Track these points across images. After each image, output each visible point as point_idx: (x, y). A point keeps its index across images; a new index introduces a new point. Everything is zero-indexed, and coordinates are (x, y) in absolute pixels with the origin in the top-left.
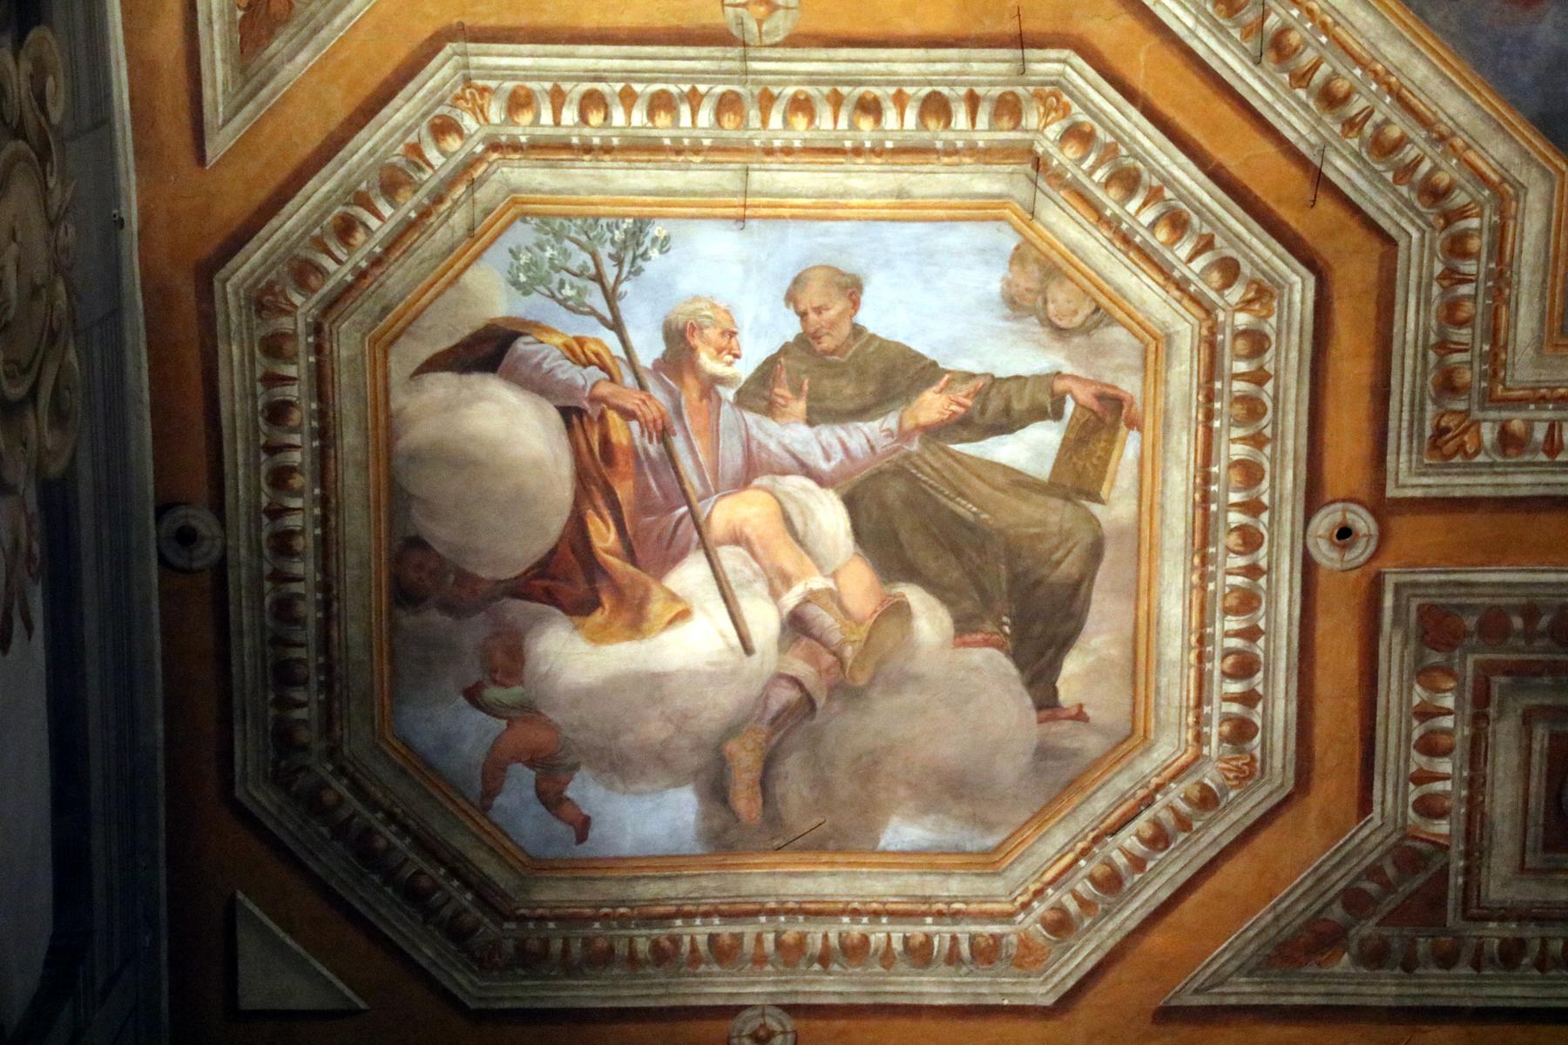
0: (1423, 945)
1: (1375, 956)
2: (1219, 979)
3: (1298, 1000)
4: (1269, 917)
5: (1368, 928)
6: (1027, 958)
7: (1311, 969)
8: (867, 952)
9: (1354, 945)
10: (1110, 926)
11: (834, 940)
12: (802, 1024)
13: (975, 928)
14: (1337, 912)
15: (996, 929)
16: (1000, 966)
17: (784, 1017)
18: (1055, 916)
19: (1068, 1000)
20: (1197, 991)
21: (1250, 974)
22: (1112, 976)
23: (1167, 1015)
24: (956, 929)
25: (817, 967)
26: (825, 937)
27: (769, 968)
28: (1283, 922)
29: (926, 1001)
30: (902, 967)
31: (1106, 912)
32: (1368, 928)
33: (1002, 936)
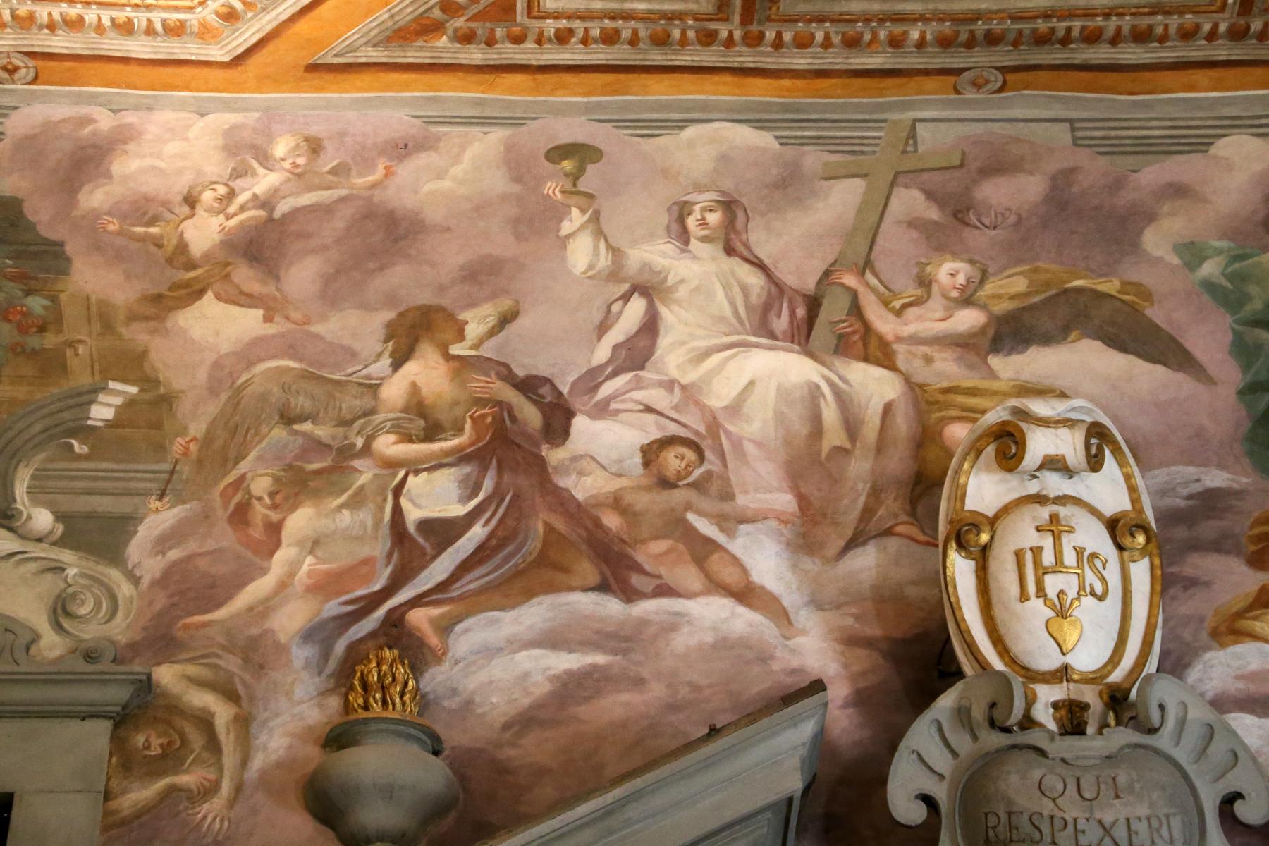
0: (499, 32)
1: (467, 38)
2: (352, 49)
3: (411, 60)
4: (386, 16)
5: (460, 23)
6: (205, 34)
7: (420, 43)
8: (84, 25)
9: (450, 32)
10: (268, 17)
11: (56, 16)
12: (40, 63)
13: (165, 15)
14: (437, 13)
15: (182, 16)
16: (185, 38)
17: (26, 59)
18: (225, 10)
19: (238, 60)
20: (335, 55)
21: (374, 46)
22: (271, 47)
23: (313, 68)
24: (150, 15)
25: (46, 31)
26: (50, 14)
27: (8, 30)
28: (397, 18)
29: (133, 55)
30: (113, 35)
31: (264, 10)
32: (460, 23)
33: (186, 21)
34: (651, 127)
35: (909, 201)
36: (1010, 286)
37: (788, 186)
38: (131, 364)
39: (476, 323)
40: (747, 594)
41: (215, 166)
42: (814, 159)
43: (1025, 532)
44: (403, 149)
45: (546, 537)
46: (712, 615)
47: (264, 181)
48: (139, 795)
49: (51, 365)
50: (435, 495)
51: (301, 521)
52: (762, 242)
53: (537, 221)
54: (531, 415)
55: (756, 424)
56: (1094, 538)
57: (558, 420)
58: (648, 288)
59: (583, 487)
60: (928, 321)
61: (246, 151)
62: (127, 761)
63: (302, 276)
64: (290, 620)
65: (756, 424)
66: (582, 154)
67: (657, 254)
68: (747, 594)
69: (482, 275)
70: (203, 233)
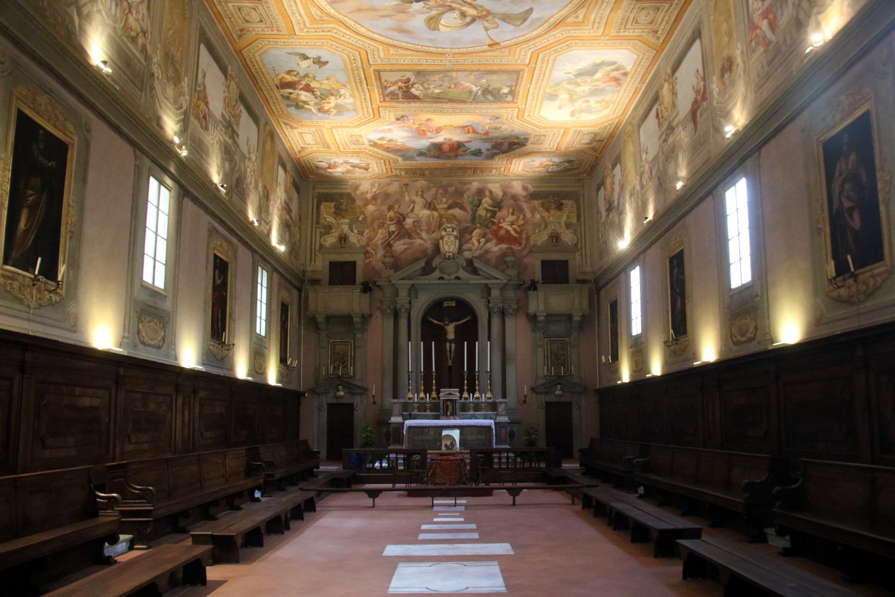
34: (414, 181)
35: (441, 191)
36: (450, 201)
37: (429, 189)
38: (362, 213)
39: (396, 207)
40: (422, 239)
41: (370, 188)
42: (432, 185)
43: (446, 238)
44: (389, 184)
45: (404, 233)
46: (419, 241)
47: (375, 189)
48: (367, 261)
49: (355, 213)
50: (393, 228)
51: (380, 231)
52: (425, 196)
53: (402, 194)
54: (402, 218)
55: (424, 219)
56: (452, 238)
57: (404, 220)
58: (414, 202)
59: (407, 227)
60: (441, 206)
61: (373, 185)
62: (366, 258)
63: (379, 201)
64: (379, 242)
65: (424, 219)
66: (406, 185)
67: (414, 198)
68: (422, 239)
69: (397, 201)
70: (369, 196)
